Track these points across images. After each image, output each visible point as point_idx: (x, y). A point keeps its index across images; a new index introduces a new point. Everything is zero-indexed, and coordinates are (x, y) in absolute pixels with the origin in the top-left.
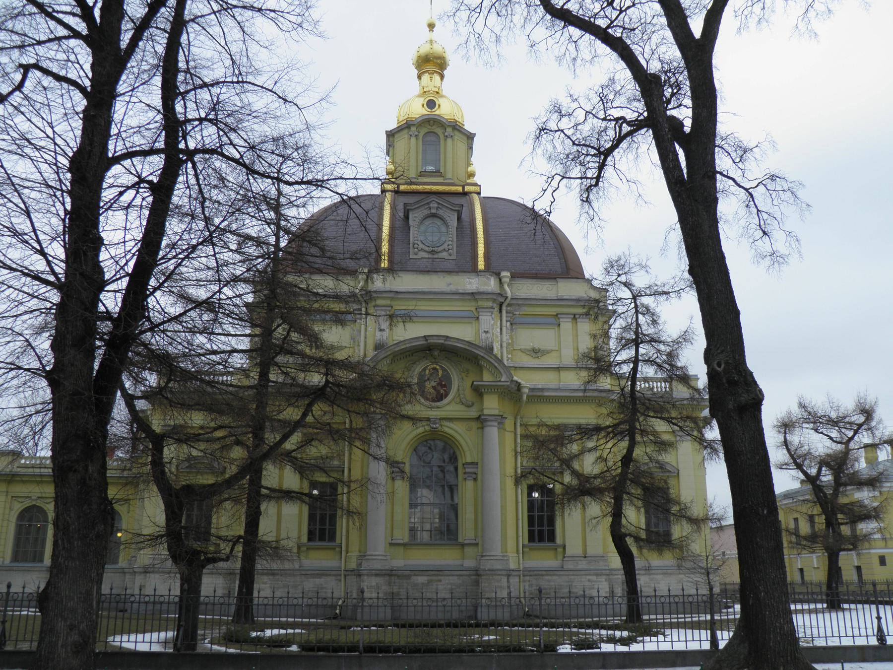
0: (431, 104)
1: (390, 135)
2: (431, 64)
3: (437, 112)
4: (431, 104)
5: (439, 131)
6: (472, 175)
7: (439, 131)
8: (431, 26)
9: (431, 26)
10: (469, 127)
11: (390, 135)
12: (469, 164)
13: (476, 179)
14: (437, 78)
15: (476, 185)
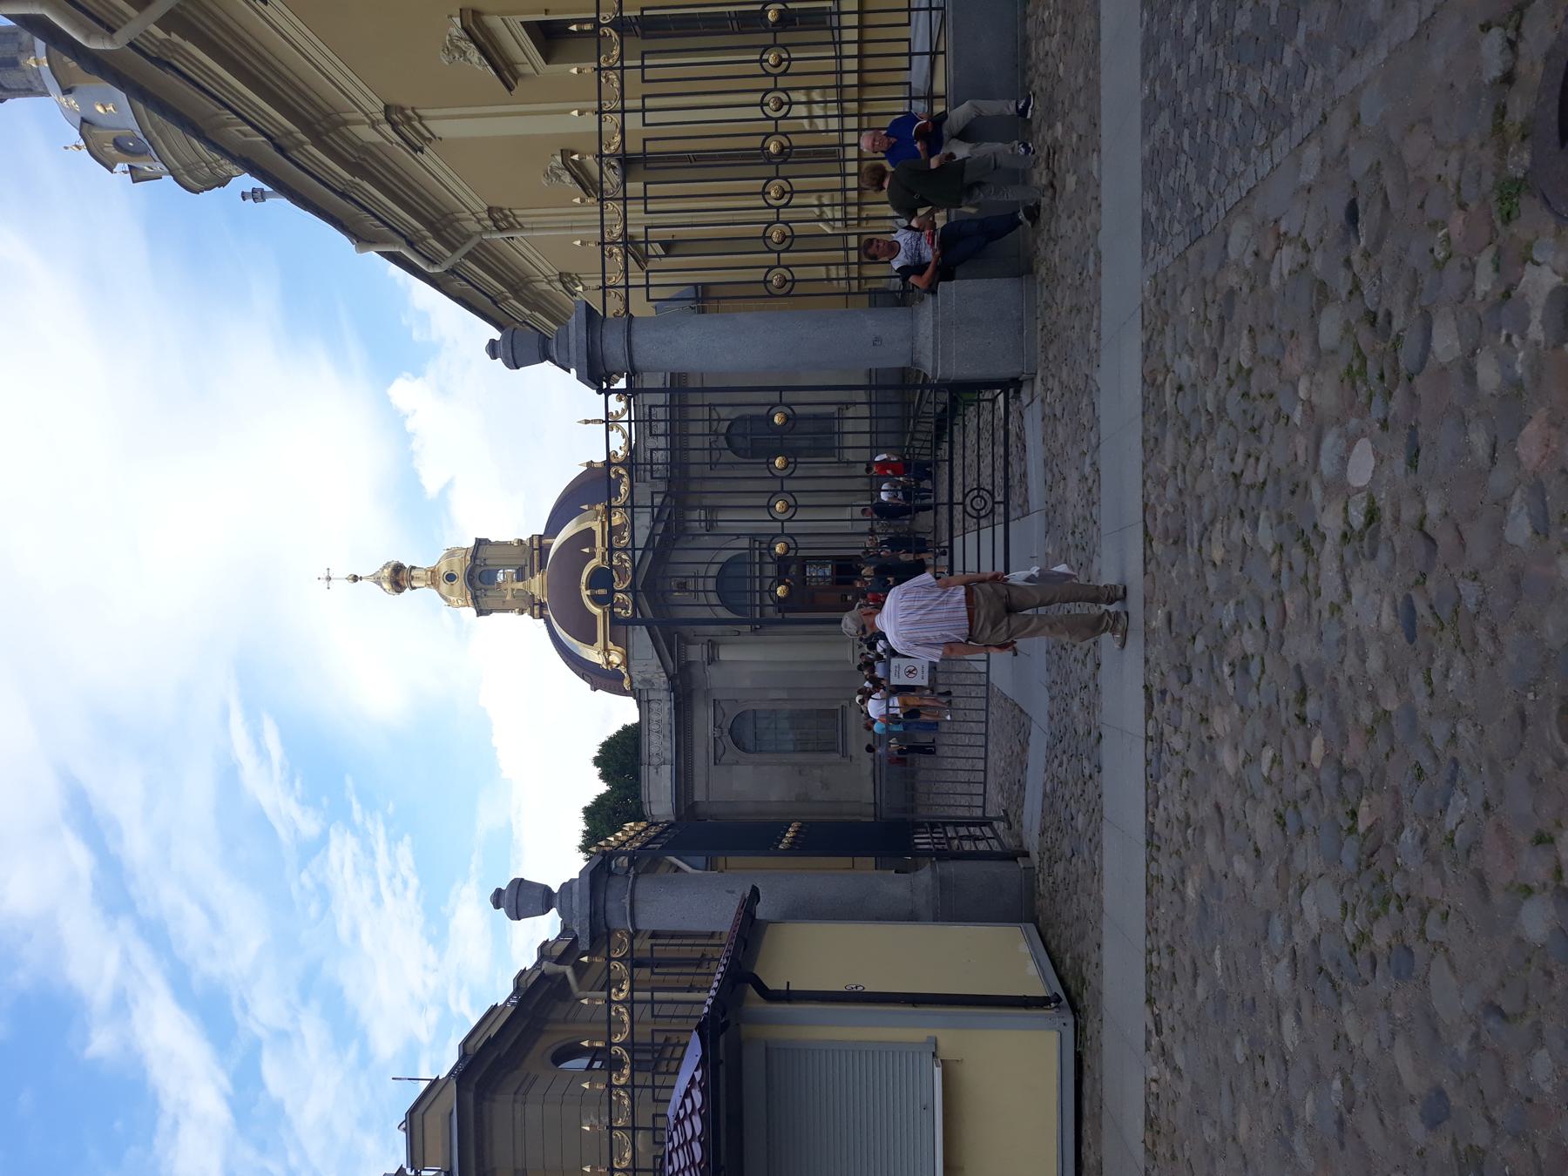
0: (450, 577)
1: (480, 613)
2: (399, 578)
3: (459, 571)
4: (450, 577)
5: (478, 570)
6: (520, 541)
7: (478, 570)
8: (355, 578)
9: (355, 578)
10: (471, 544)
11: (480, 613)
12: (511, 544)
13: (525, 537)
14: (414, 573)
15: (531, 539)
